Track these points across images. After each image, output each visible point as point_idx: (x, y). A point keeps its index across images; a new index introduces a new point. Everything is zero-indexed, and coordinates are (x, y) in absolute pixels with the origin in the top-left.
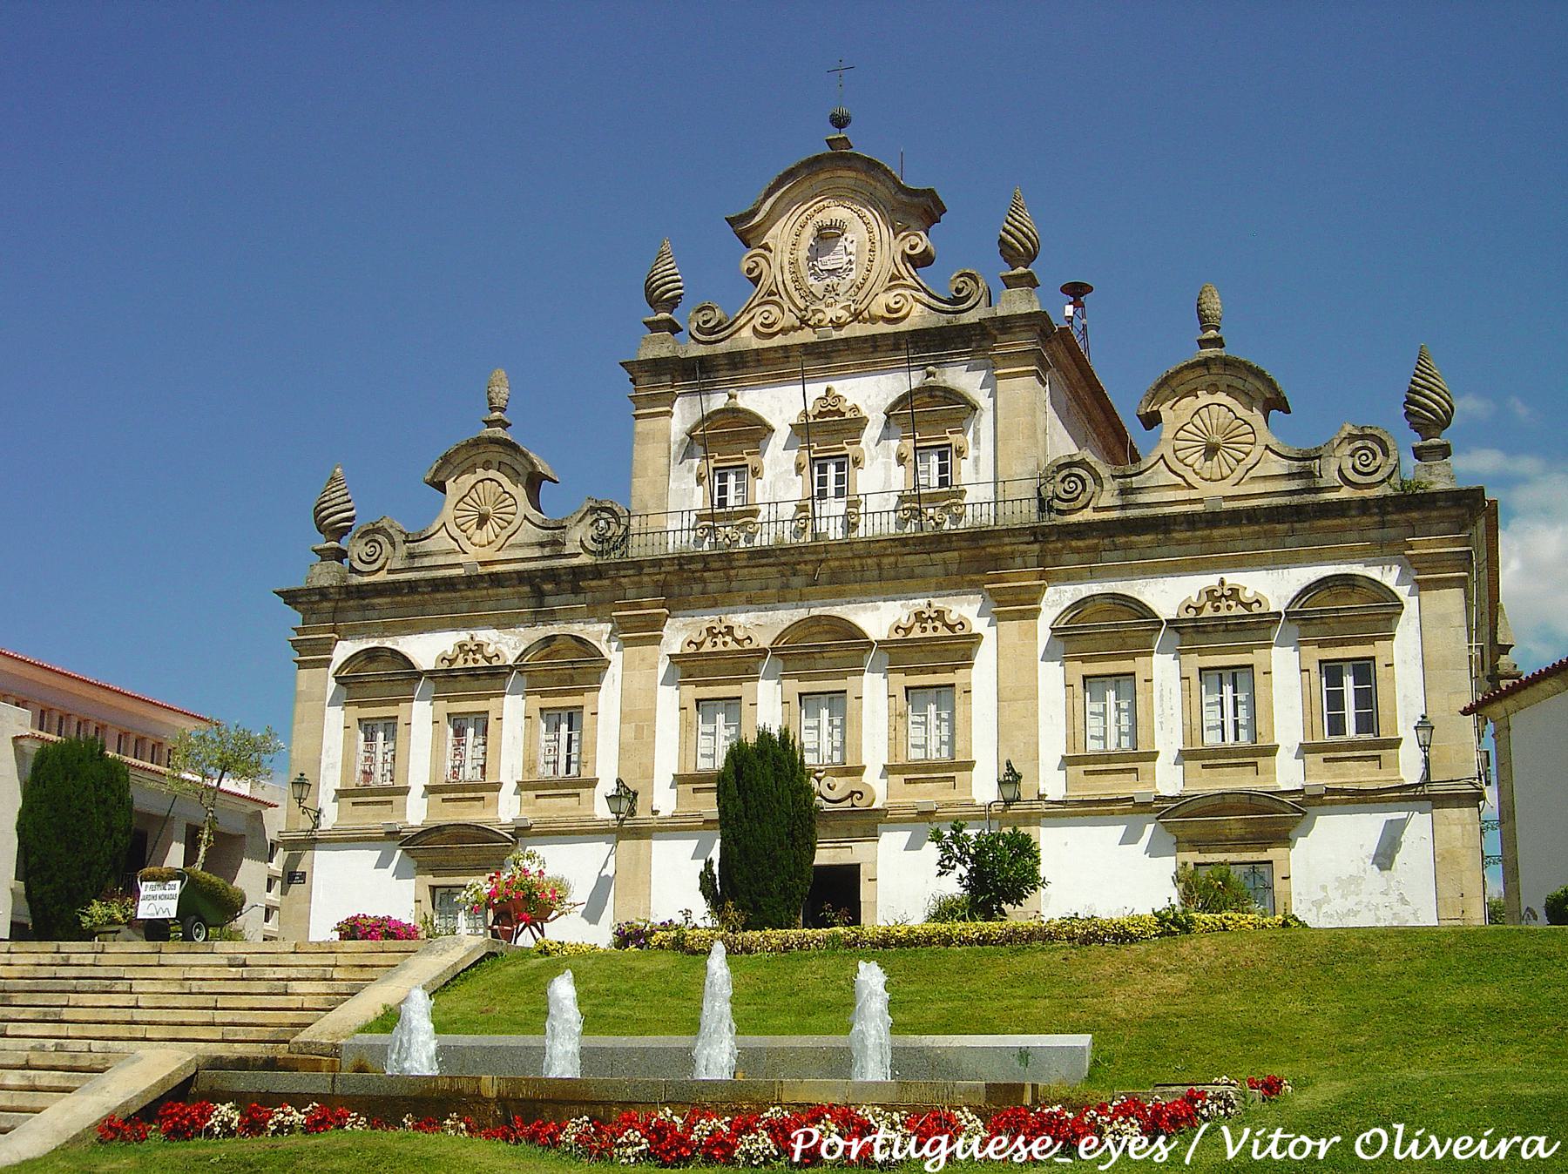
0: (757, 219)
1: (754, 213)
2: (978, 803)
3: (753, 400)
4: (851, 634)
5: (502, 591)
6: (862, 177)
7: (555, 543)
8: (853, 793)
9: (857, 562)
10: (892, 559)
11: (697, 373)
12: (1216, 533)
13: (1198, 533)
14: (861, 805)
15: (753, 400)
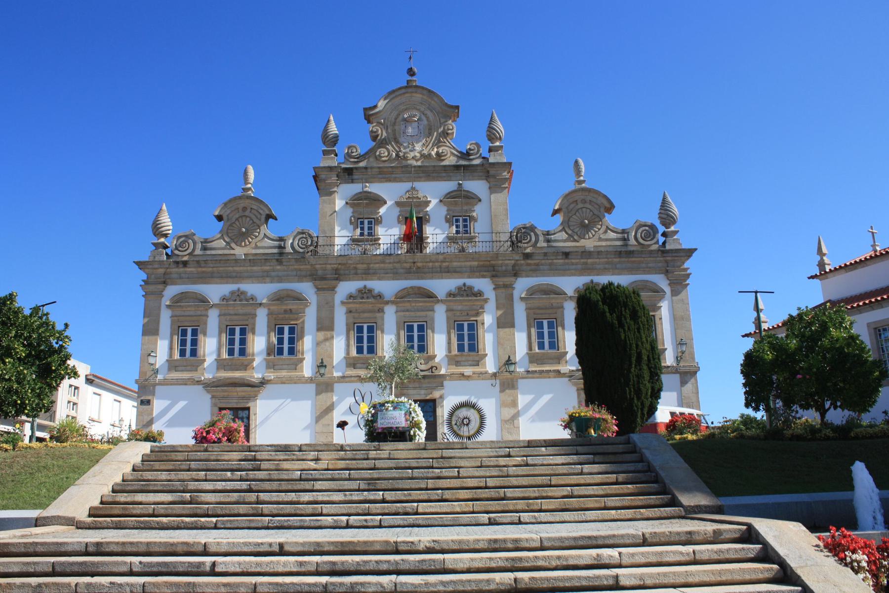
0: (377, 110)
1: (375, 107)
2: (490, 372)
3: (375, 188)
4: (429, 295)
5: (255, 268)
6: (425, 97)
7: (280, 247)
8: (432, 368)
9: (431, 264)
10: (447, 264)
11: (348, 174)
12: (590, 261)
13: (582, 260)
14: (436, 373)
15: (375, 188)
